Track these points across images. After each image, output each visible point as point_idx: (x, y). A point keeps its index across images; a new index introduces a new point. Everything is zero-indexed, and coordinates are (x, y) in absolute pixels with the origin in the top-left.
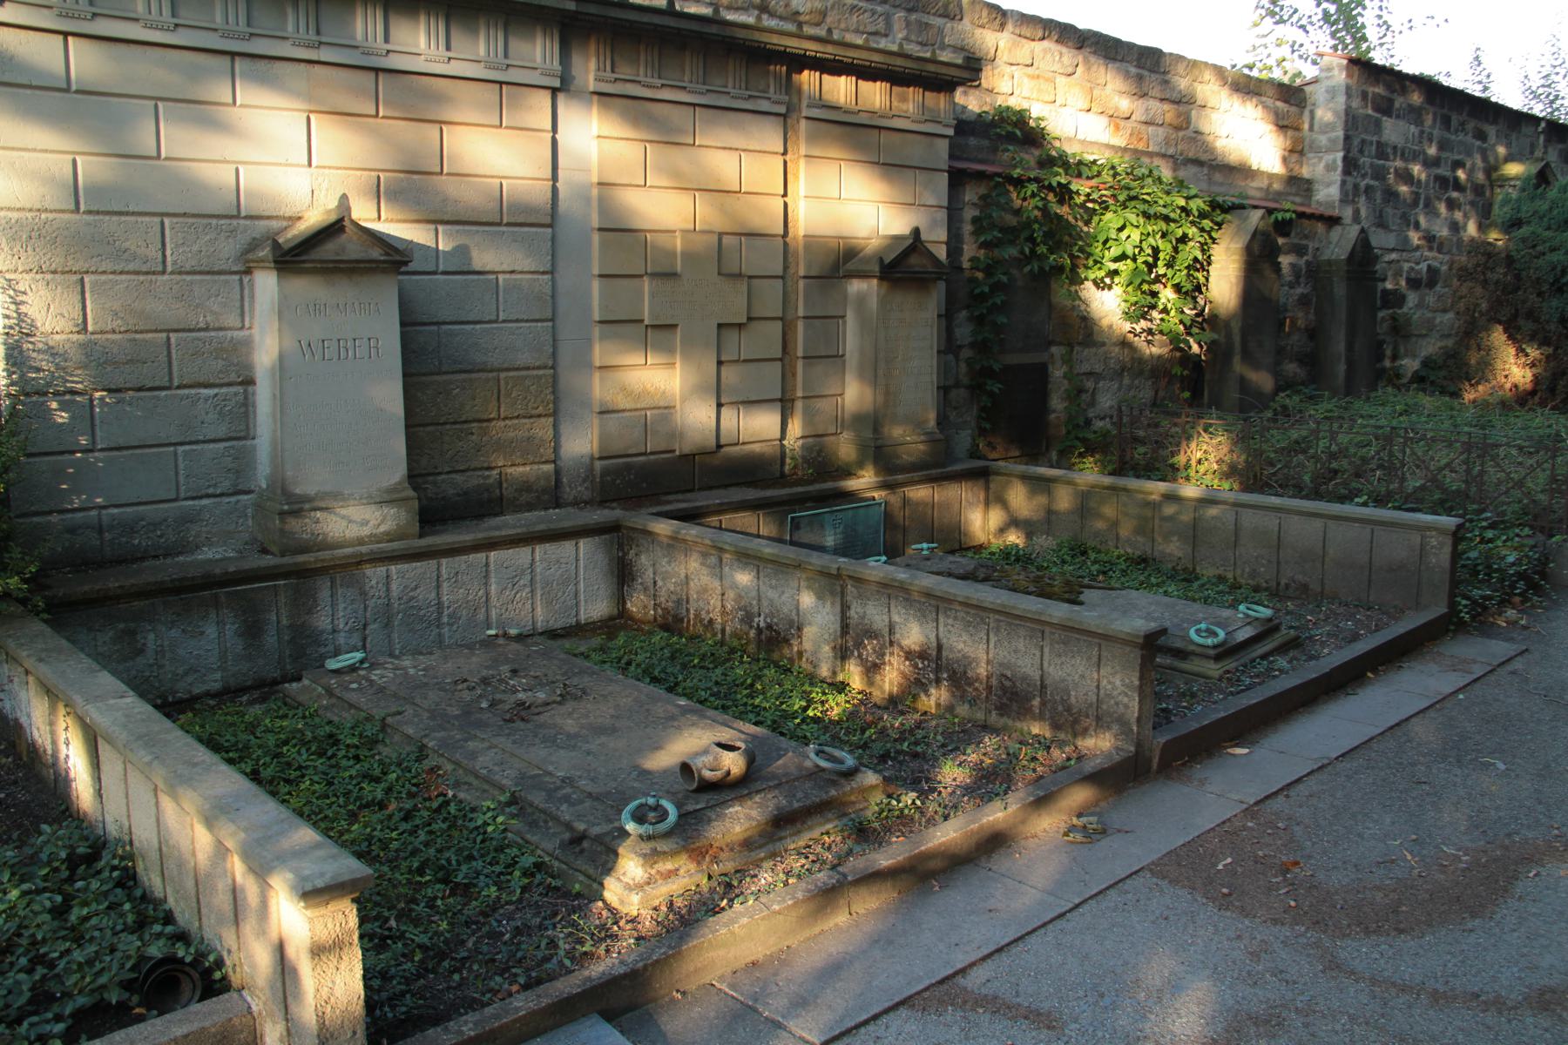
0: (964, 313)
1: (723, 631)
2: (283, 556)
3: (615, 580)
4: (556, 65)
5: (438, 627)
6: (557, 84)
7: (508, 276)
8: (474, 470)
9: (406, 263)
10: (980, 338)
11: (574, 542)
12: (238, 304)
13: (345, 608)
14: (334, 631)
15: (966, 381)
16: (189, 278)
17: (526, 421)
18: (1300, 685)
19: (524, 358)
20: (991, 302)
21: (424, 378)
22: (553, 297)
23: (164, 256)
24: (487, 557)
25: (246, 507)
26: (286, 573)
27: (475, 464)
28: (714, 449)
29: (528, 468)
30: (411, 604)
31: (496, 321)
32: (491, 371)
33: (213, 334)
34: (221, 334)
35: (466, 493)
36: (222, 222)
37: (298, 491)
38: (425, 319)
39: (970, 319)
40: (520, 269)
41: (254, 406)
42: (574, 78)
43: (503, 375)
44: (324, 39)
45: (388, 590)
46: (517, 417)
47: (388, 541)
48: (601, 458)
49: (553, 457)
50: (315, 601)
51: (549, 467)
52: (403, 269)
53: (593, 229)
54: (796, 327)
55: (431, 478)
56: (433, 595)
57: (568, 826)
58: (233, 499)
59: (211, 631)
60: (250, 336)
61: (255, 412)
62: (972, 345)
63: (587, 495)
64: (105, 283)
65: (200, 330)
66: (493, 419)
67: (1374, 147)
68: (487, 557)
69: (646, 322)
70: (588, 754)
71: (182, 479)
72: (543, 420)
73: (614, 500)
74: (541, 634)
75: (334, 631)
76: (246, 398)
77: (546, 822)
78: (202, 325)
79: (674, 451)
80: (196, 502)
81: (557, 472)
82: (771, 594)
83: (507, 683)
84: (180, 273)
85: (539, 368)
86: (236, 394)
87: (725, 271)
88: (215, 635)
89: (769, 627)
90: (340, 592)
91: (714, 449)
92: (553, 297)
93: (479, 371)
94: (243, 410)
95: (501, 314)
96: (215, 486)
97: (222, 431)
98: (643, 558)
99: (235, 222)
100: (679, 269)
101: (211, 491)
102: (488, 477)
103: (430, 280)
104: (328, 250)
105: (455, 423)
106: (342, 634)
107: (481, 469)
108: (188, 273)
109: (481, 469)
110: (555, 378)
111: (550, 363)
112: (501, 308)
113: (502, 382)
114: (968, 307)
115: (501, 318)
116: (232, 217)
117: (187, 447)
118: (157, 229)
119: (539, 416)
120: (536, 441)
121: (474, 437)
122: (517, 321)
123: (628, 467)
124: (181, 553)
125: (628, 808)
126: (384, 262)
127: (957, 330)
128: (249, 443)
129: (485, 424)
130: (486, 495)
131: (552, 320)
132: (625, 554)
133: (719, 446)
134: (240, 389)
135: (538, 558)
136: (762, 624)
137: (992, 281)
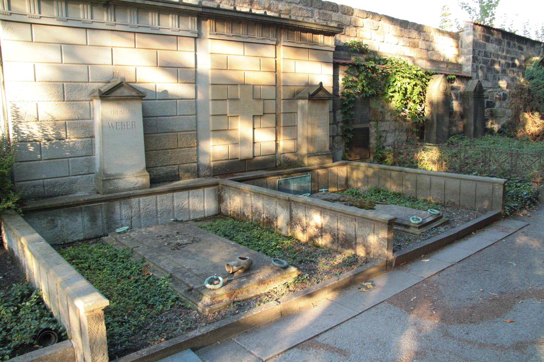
0: (340, 111)
1: (252, 219)
2: (104, 194)
3: (217, 202)
4: (196, 30)
5: (156, 218)
6: (196, 36)
7: (180, 100)
8: (170, 165)
9: (144, 97)
10: (345, 119)
11: (203, 189)
12: (89, 111)
13: (125, 212)
14: (121, 219)
15: (341, 134)
16: (72, 103)
17: (187, 149)
19: (186, 127)
20: (348, 107)
21: (152, 135)
22: (196, 107)
23: (64, 96)
24: (173, 195)
25: (92, 178)
26: (105, 201)
27: (170, 163)
28: (252, 158)
29: (188, 165)
30: (147, 210)
31: (176, 115)
32: (175, 132)
33: (80, 121)
34: (83, 121)
35: (167, 173)
36: (83, 84)
37: (109, 173)
38: (152, 115)
39: (342, 113)
41: (94, 145)
42: (202, 34)
43: (179, 133)
44: (116, 23)
45: (139, 206)
46: (184, 147)
47: (139, 189)
48: (213, 161)
49: (196, 161)
50: (115, 209)
51: (195, 164)
52: (144, 98)
53: (209, 84)
54: (280, 116)
55: (155, 168)
56: (155, 207)
57: (188, 285)
58: (88, 176)
59: (80, 219)
60: (93, 121)
61: (95, 147)
62: (342, 122)
63: (208, 174)
65: (76, 120)
66: (176, 148)
67: (483, 53)
68: (173, 195)
69: (228, 115)
70: (198, 261)
71: (71, 169)
72: (193, 148)
73: (217, 175)
74: (192, 220)
75: (121, 219)
76: (92, 142)
77: (181, 284)
78: (77, 118)
79: (238, 158)
80: (75, 177)
81: (198, 166)
82: (267, 206)
83: (175, 237)
84: (69, 101)
85: (191, 131)
86: (88, 141)
87: (255, 97)
88: (81, 221)
89: (267, 218)
90: (123, 206)
91: (252, 158)
92: (196, 107)
93: (171, 132)
94: (91, 146)
95: (178, 113)
96: (82, 171)
97: (84, 153)
98: (226, 194)
99: (87, 84)
100: (239, 97)
101: (80, 173)
102: (174, 167)
103: (154, 102)
104: (118, 92)
105: (163, 150)
106: (124, 220)
107: (172, 165)
108: (72, 101)
109: (172, 165)
110: (197, 134)
111: (195, 129)
112: (178, 111)
113: (179, 136)
114: (341, 109)
115: (178, 115)
117: (72, 159)
119: (192, 147)
120: (191, 156)
121: (169, 154)
122: (184, 115)
123: (223, 164)
124: (70, 194)
125: (207, 279)
126: (137, 96)
127: (337, 117)
128: (93, 157)
129: (173, 150)
130: (173, 174)
131: (196, 115)
132: (221, 193)
133: (254, 157)
134: (90, 139)
135: (190, 195)
136: (265, 217)
137: (349, 100)
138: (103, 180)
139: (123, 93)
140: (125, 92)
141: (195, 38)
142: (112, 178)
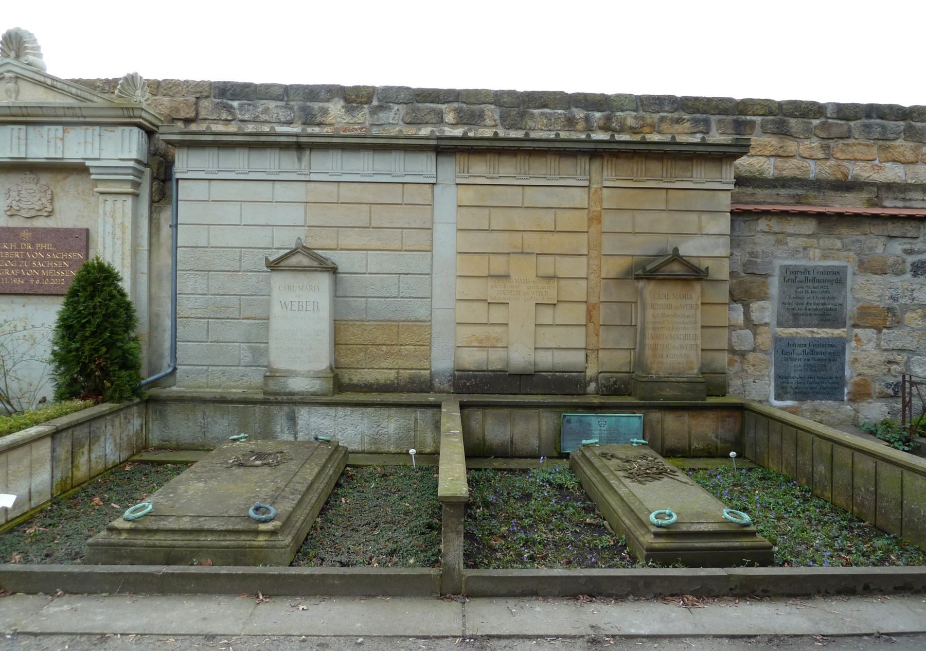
6: (433, 181)
18: (662, 576)
37: (275, 367)
40: (412, 272)
48: (457, 370)
55: (359, 370)
104: (294, 260)
122: (410, 297)
131: (431, 298)
138: (265, 376)
139: (301, 263)
140: (305, 261)
141: (434, 184)
142: (277, 374)
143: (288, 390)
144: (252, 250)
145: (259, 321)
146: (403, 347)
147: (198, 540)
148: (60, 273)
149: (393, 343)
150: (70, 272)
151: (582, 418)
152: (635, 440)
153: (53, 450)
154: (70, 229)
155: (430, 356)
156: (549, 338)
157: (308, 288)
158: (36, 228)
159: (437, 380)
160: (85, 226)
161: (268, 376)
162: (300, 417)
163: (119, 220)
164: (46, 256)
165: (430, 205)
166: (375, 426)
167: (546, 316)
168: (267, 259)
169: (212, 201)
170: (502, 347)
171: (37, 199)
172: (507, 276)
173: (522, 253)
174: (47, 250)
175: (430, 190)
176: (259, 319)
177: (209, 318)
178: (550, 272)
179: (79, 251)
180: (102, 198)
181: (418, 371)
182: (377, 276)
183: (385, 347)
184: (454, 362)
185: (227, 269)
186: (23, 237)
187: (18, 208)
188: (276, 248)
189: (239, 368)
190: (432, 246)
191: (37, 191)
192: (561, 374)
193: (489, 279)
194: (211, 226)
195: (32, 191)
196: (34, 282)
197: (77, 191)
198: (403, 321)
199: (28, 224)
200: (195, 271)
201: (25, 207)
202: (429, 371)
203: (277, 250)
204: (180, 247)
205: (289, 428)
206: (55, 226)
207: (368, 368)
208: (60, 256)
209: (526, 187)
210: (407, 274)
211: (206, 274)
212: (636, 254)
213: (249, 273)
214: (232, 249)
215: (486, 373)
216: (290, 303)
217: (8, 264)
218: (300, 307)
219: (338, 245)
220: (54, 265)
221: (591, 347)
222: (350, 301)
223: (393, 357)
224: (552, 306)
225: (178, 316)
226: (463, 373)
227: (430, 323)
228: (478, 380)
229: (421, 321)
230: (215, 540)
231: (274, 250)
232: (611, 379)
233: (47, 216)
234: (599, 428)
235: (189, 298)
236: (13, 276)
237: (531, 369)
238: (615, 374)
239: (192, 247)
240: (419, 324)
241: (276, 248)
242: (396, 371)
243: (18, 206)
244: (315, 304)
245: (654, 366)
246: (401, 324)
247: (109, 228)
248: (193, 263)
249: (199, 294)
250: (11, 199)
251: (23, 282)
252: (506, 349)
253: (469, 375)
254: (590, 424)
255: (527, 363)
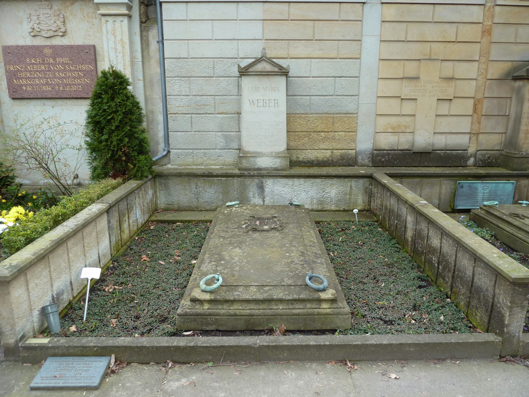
37: (247, 150)
40: (345, 75)
48: (375, 150)
64: (196, 80)
104: (260, 67)
116: (236, 58)
118: (212, 63)
122: (343, 95)
139: (265, 68)
140: (268, 67)
142: (248, 155)
143: (256, 167)
144: (222, 60)
145: (229, 115)
146: (336, 133)
147: (271, 309)
148: (77, 81)
149: (329, 131)
150: (85, 80)
151: (471, 184)
152: (525, 202)
153: (109, 222)
154: (81, 46)
155: (356, 140)
156: (445, 125)
157: (270, 89)
158: (55, 46)
159: (360, 157)
160: (92, 43)
161: (242, 157)
162: (267, 186)
163: (119, 38)
164: (65, 68)
165: (361, 21)
166: (321, 192)
167: (444, 109)
168: (239, 66)
169: (189, 20)
170: (409, 133)
171: (52, 22)
172: (417, 78)
173: (429, 59)
174: (65, 63)
175: (361, 8)
176: (229, 114)
177: (192, 114)
178: (449, 74)
179: (90, 63)
180: (104, 19)
181: (347, 151)
182: (318, 78)
183: (323, 133)
184: (373, 144)
185: (204, 75)
186: (46, 53)
187: (39, 30)
188: (240, 58)
189: (216, 150)
190: (360, 54)
191: (52, 16)
192: (450, 152)
193: (404, 80)
194: (189, 41)
195: (49, 15)
196: (59, 89)
197: (83, 14)
198: (337, 114)
199: (48, 43)
200: (180, 77)
201: (45, 28)
202: (355, 151)
203: (241, 60)
204: (167, 58)
205: (259, 194)
206: (69, 44)
207: (311, 149)
208: (76, 67)
209: (436, 6)
210: (341, 77)
211: (188, 80)
212: (516, 60)
213: (221, 79)
214: (207, 60)
215: (397, 152)
216: (257, 101)
217: (37, 75)
218: (265, 104)
219: (288, 55)
220: (72, 75)
221: (474, 132)
222: (297, 98)
223: (329, 141)
224: (449, 101)
225: (168, 112)
226: (379, 152)
227: (357, 115)
228: (390, 156)
229: (351, 114)
230: (286, 309)
231: (239, 60)
232: (486, 156)
233: (62, 36)
234: (482, 191)
235: (176, 98)
236: (42, 84)
237: (430, 148)
238: (489, 152)
239: (176, 58)
240: (348, 115)
241: (240, 58)
242: (331, 151)
243: (39, 28)
244: (276, 101)
245: (525, 146)
246: (335, 116)
247: (112, 44)
248: (177, 71)
249: (183, 96)
250: (32, 22)
251: (50, 89)
252: (412, 134)
253: (384, 153)
254: (476, 189)
255: (427, 144)
